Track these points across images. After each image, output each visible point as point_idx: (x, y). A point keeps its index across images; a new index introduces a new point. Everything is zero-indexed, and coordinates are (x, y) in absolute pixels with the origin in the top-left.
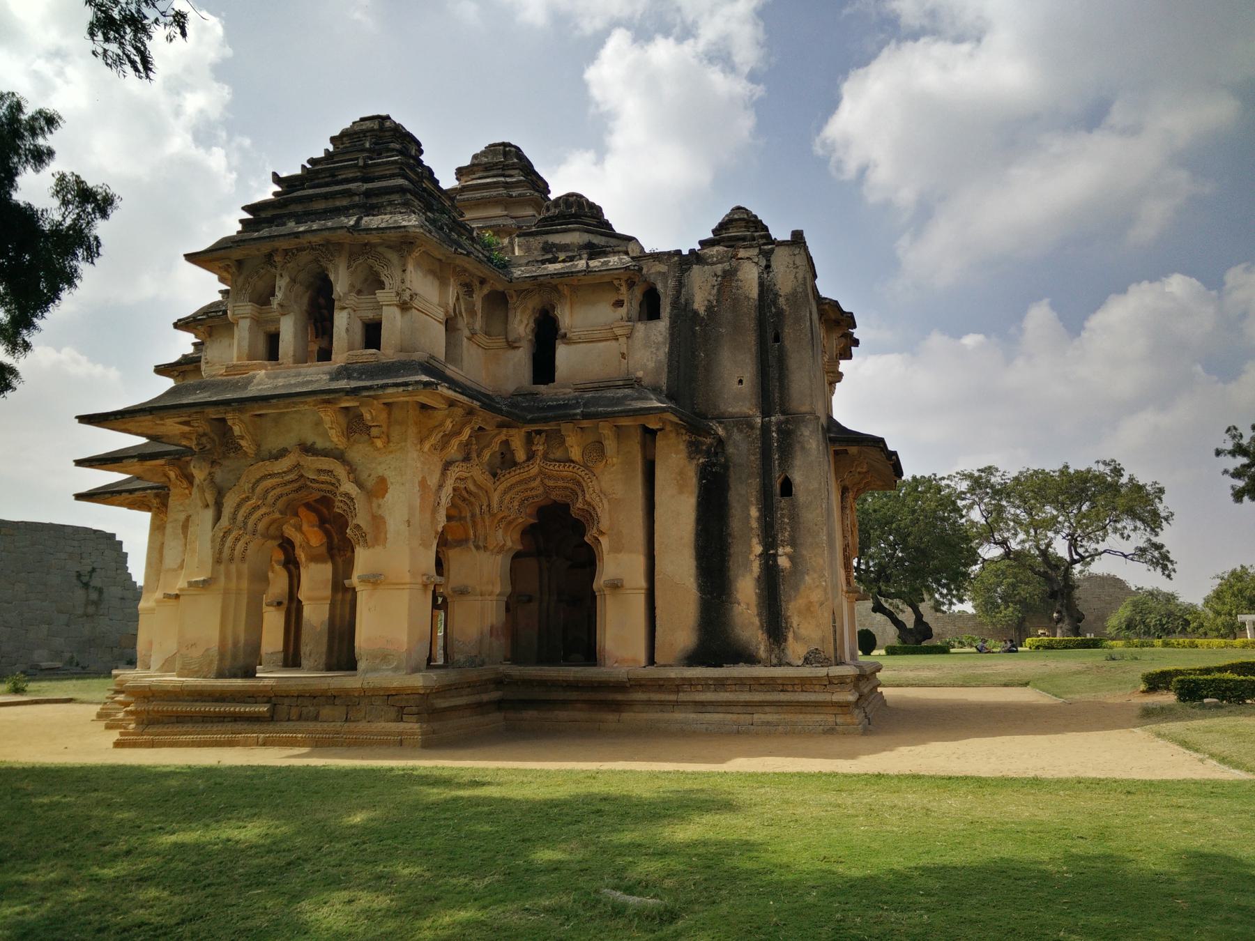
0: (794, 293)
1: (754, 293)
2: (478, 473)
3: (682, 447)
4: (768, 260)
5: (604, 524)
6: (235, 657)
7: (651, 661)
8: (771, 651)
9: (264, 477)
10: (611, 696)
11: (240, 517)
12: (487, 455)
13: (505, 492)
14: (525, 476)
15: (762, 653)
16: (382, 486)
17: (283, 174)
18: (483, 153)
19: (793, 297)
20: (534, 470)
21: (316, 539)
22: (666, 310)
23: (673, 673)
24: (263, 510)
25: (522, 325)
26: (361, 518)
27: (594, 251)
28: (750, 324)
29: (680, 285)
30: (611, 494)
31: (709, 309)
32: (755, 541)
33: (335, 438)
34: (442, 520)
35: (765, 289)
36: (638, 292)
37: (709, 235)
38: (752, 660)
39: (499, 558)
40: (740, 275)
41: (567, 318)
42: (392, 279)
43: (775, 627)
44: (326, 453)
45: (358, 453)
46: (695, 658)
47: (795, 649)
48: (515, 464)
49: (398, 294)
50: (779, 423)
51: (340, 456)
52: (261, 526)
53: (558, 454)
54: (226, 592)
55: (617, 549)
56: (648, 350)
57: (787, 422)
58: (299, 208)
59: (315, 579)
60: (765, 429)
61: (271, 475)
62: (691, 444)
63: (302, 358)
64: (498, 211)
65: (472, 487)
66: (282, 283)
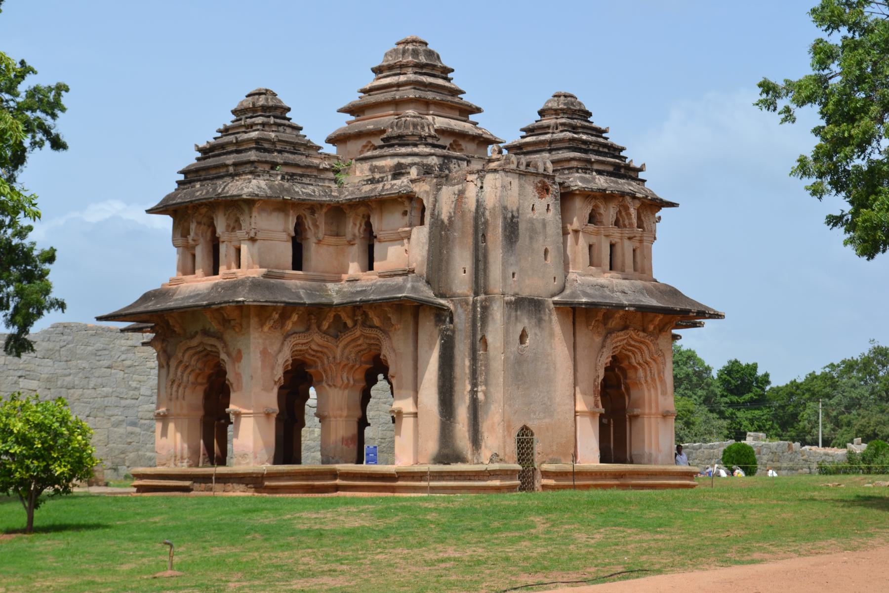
1: (472, 206)
3: (432, 318)
8: (473, 454)
14: (353, 337)
15: (469, 456)
16: (238, 357)
17: (200, 146)
28: (470, 230)
29: (436, 201)
31: (450, 218)
32: (467, 382)
35: (479, 204)
37: (532, 118)
39: (346, 392)
41: (376, 226)
47: (485, 454)
49: (247, 233)
50: (481, 302)
51: (220, 337)
57: (486, 300)
60: (474, 304)
65: (314, 347)
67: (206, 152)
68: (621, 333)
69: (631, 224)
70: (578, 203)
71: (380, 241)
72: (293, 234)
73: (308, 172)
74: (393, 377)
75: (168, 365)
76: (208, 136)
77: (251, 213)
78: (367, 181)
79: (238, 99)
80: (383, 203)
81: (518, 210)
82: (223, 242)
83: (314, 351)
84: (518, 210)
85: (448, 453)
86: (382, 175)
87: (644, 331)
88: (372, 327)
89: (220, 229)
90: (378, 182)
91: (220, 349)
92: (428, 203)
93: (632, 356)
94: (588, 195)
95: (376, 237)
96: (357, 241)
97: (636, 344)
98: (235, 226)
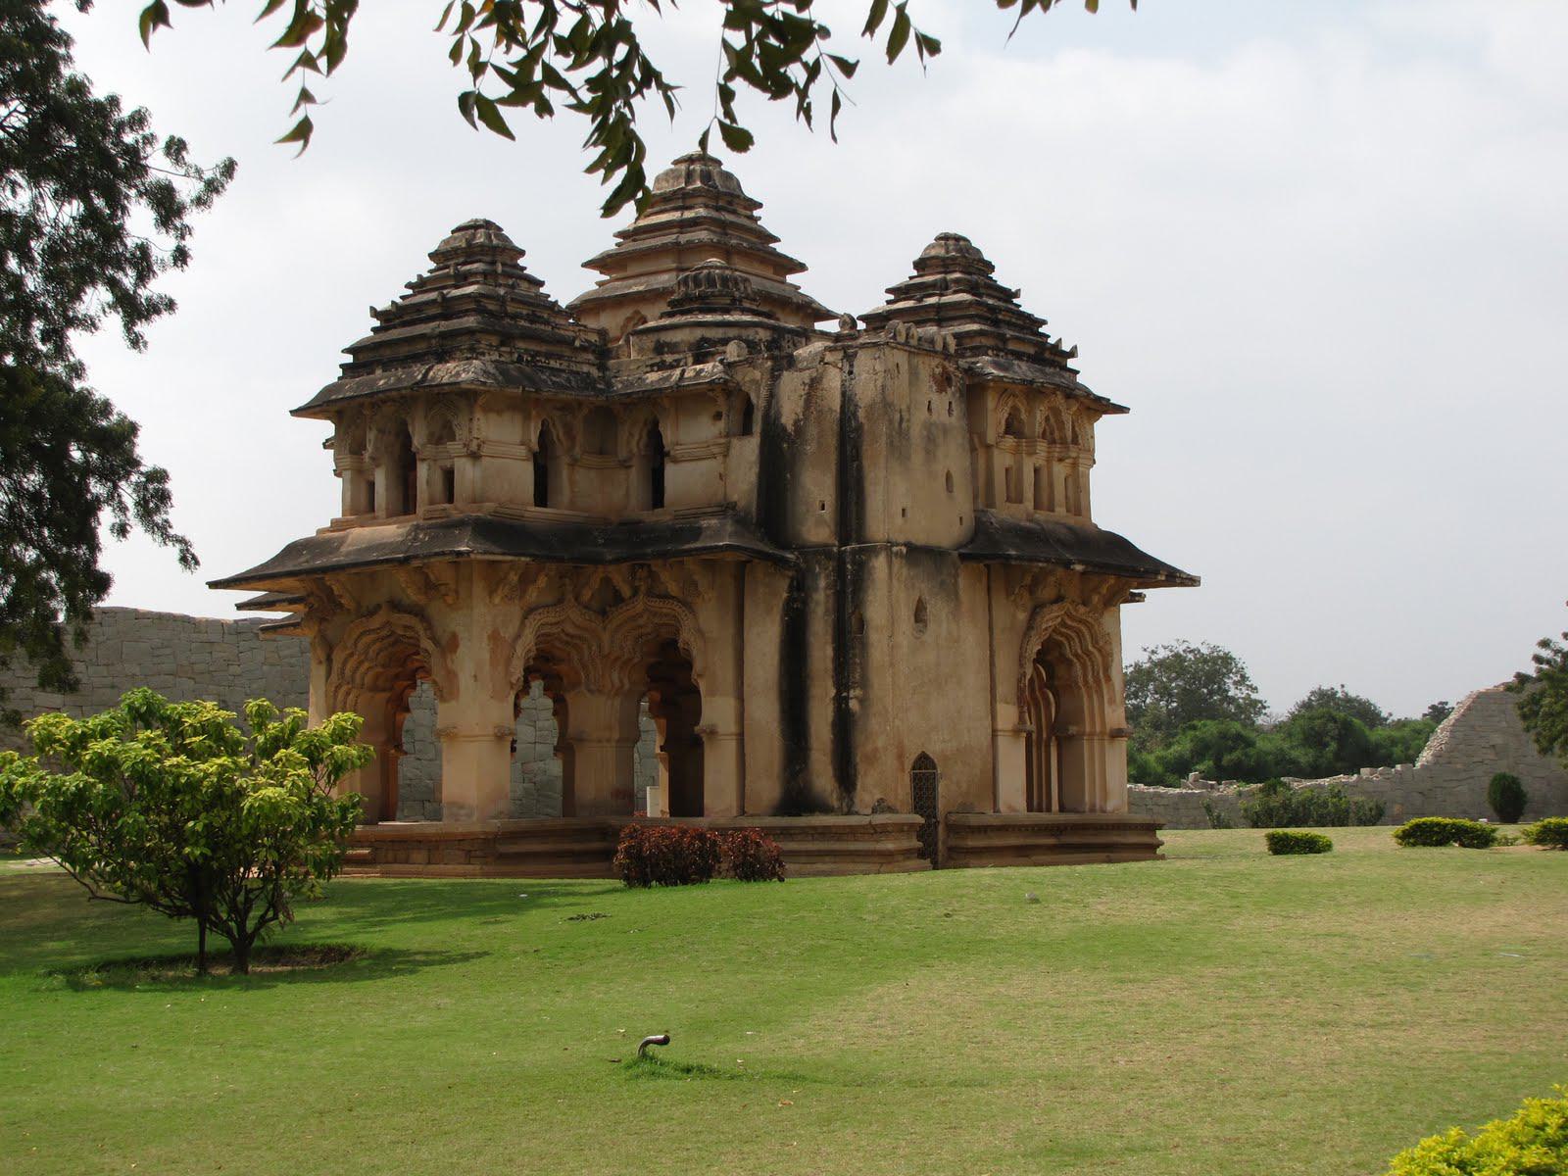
1: (836, 404)
4: (851, 366)
7: (742, 812)
8: (841, 799)
9: (360, 637)
11: (348, 672)
15: (834, 801)
16: (453, 644)
20: (639, 606)
22: (757, 428)
24: (366, 665)
25: (631, 441)
28: (832, 442)
29: (772, 395)
30: (705, 632)
31: (796, 423)
33: (413, 596)
35: (847, 398)
37: (904, 274)
38: (827, 810)
39: (617, 702)
40: (825, 383)
41: (668, 436)
43: (846, 777)
48: (623, 600)
49: (465, 445)
50: (854, 552)
51: (419, 612)
52: (368, 680)
55: (712, 693)
58: (388, 353)
61: (370, 631)
64: (670, 263)
65: (570, 630)
66: (371, 436)
67: (388, 318)
68: (1055, 607)
69: (1063, 442)
70: (991, 402)
71: (675, 461)
72: (536, 448)
73: (556, 349)
74: (699, 676)
75: (329, 660)
76: (391, 292)
77: (472, 412)
78: (652, 366)
79: (438, 234)
80: (687, 399)
81: (909, 408)
82: (423, 460)
83: (567, 635)
84: (909, 408)
85: (797, 799)
86: (677, 356)
87: (1084, 604)
88: (666, 597)
89: (418, 440)
90: (672, 367)
91: (421, 632)
92: (759, 400)
93: (1066, 642)
94: (1004, 389)
95: (668, 454)
96: (635, 462)
97: (1074, 624)
98: (443, 435)
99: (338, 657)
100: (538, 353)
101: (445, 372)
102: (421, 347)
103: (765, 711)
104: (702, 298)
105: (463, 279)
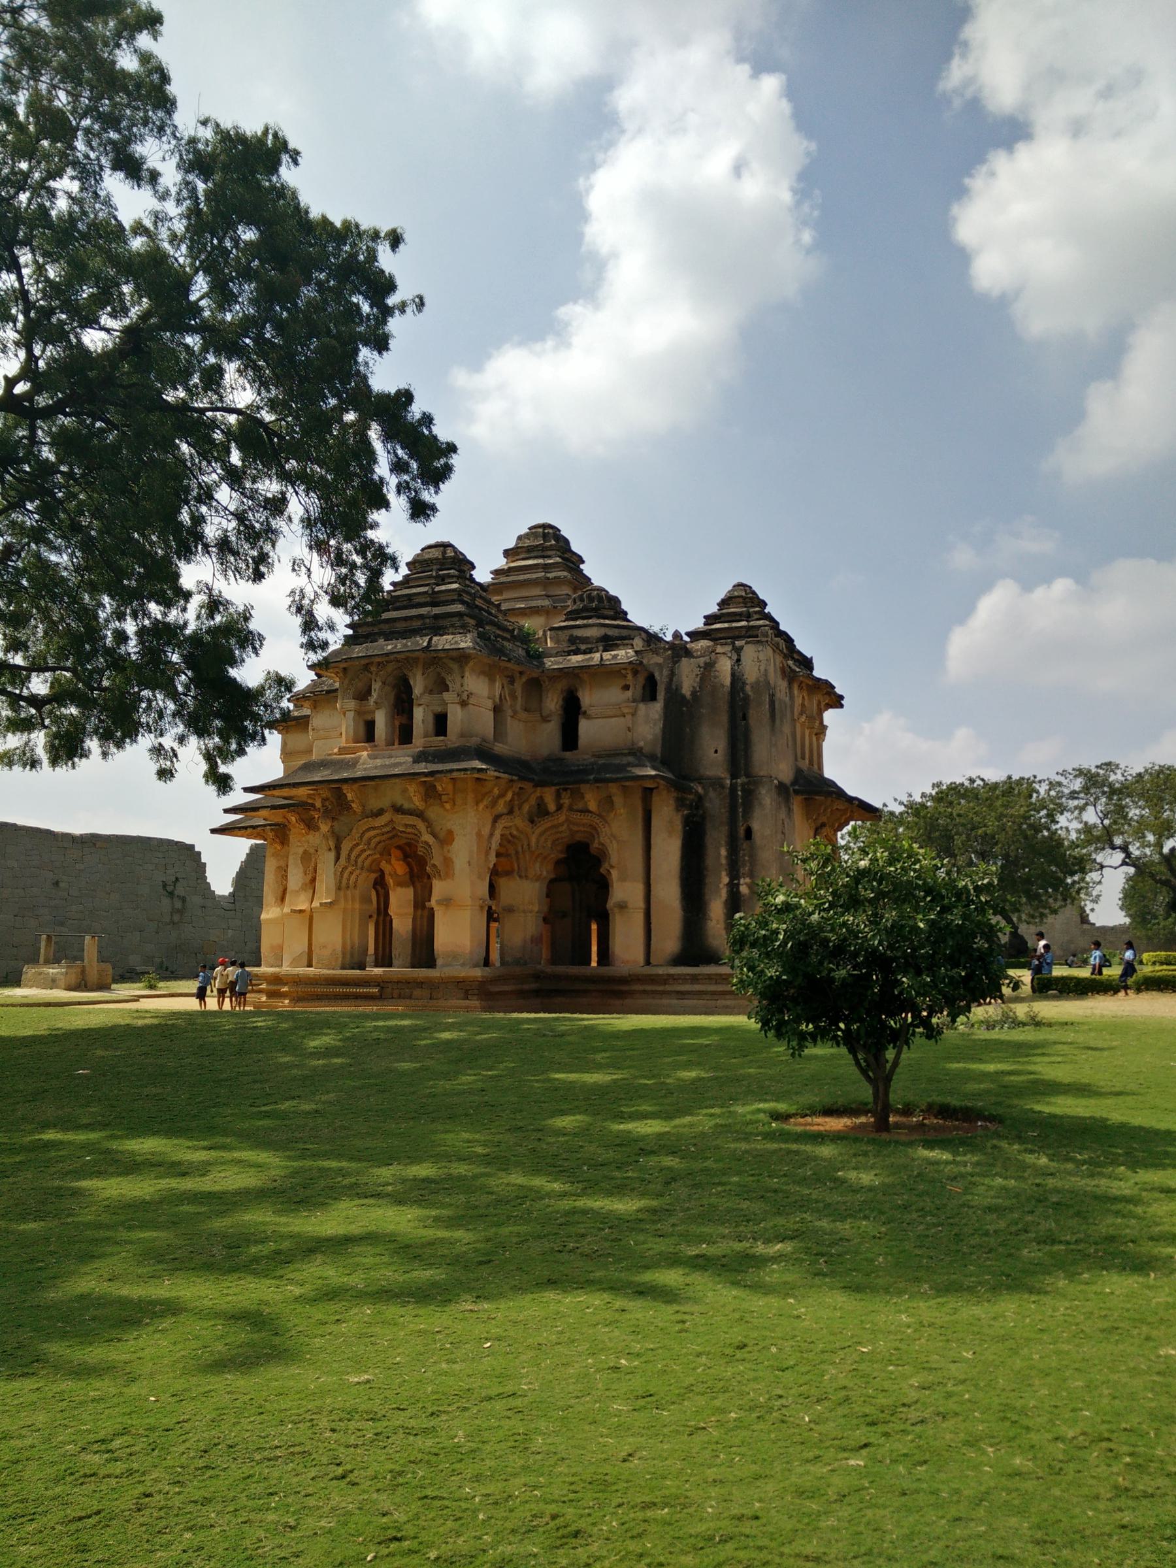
0: (757, 683)
2: (519, 822)
3: (672, 802)
4: (739, 655)
5: (614, 858)
6: (352, 955)
7: (648, 962)
9: (368, 830)
10: (616, 988)
11: (353, 857)
12: (526, 807)
13: (541, 835)
14: (556, 822)
18: (526, 536)
19: (756, 686)
20: (562, 818)
21: (400, 868)
22: (661, 694)
23: (660, 971)
24: (369, 852)
25: (553, 703)
26: (437, 860)
27: (608, 643)
28: (724, 706)
29: (672, 674)
30: (619, 839)
31: (694, 693)
32: (724, 873)
33: (418, 803)
34: (493, 859)
35: (736, 678)
36: (641, 679)
37: (714, 609)
39: (537, 884)
41: (587, 698)
42: (453, 683)
44: (410, 813)
45: (433, 812)
46: (678, 960)
48: (547, 813)
50: (743, 785)
51: (420, 815)
52: (367, 863)
53: (580, 806)
54: (345, 911)
55: (623, 879)
56: (647, 725)
57: (749, 783)
58: (386, 628)
59: (400, 900)
60: (733, 788)
61: (374, 828)
62: (677, 800)
63: (390, 743)
64: (537, 591)
66: (376, 686)
71: (589, 718)
75: (338, 849)
89: (417, 690)
92: (661, 678)
99: (346, 847)
100: (499, 636)
101: (443, 642)
102: (417, 624)
103: (668, 891)
104: (596, 609)
105: (442, 580)
